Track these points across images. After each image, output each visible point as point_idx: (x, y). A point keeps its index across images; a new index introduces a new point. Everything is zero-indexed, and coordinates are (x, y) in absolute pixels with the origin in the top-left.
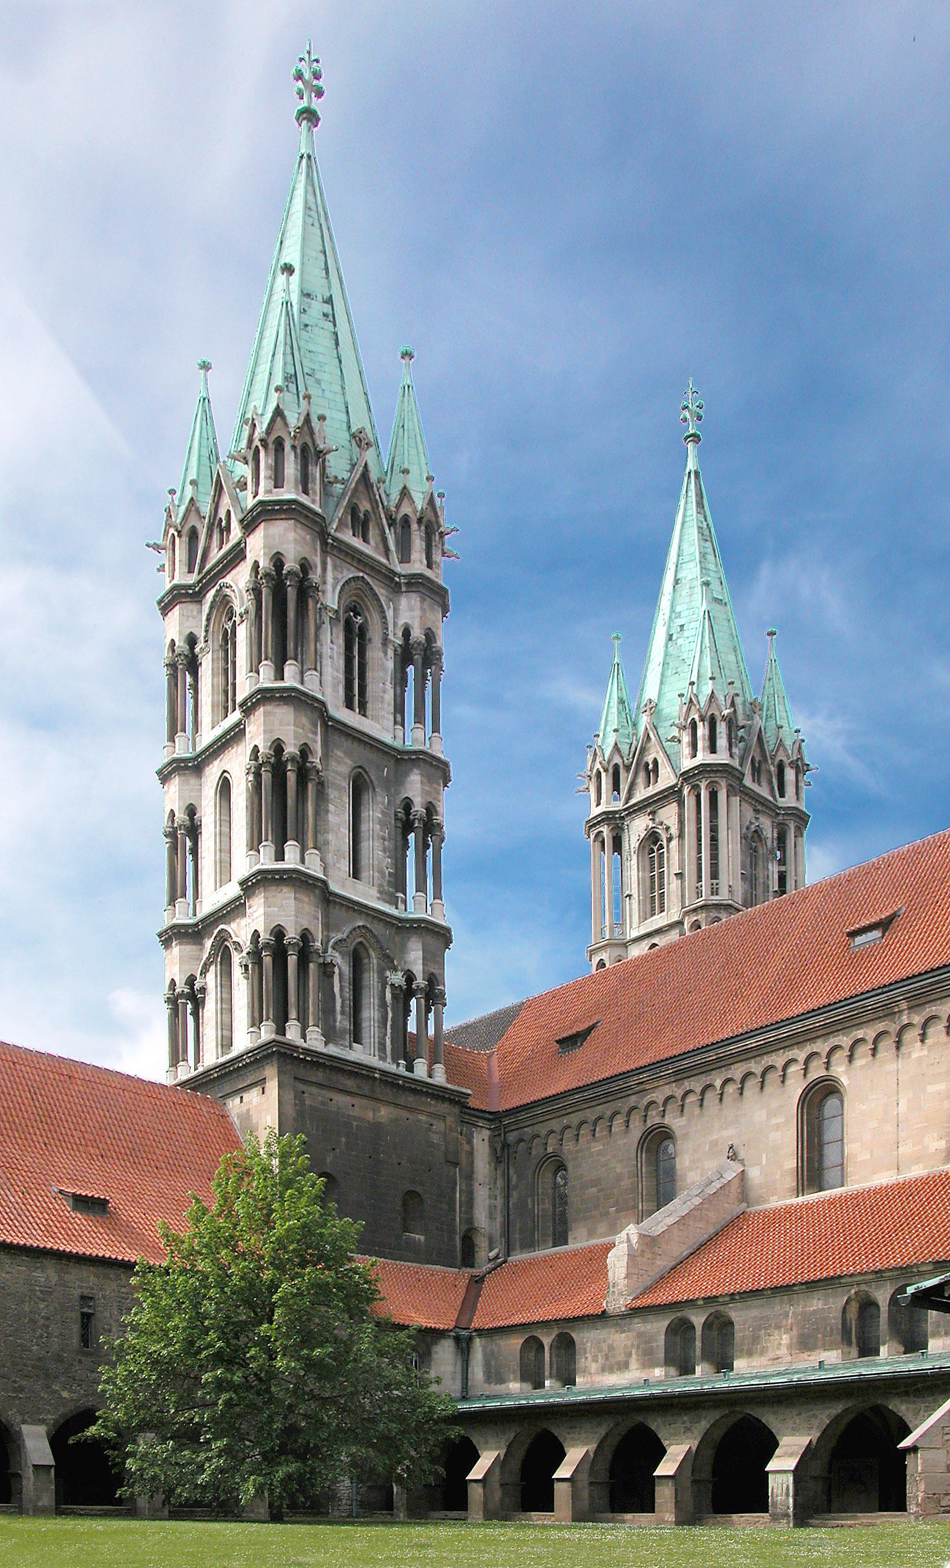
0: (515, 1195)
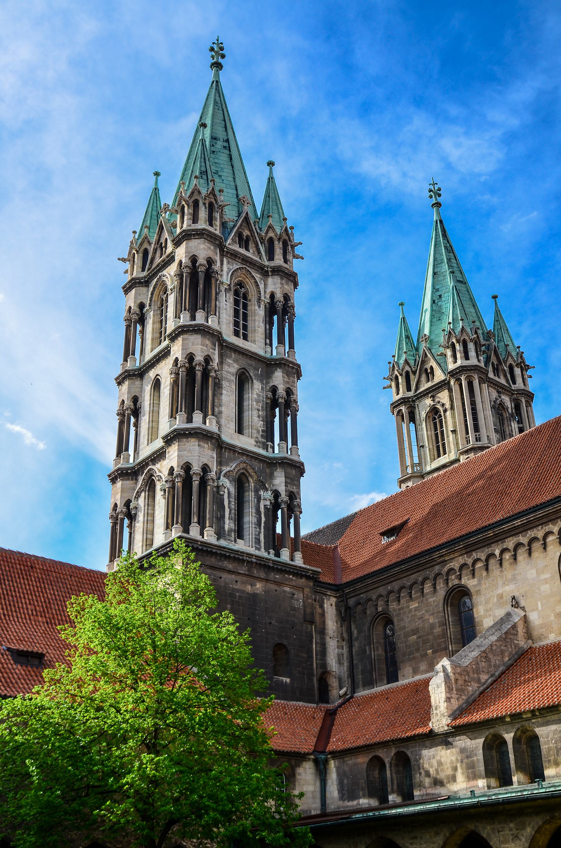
0: (356, 644)
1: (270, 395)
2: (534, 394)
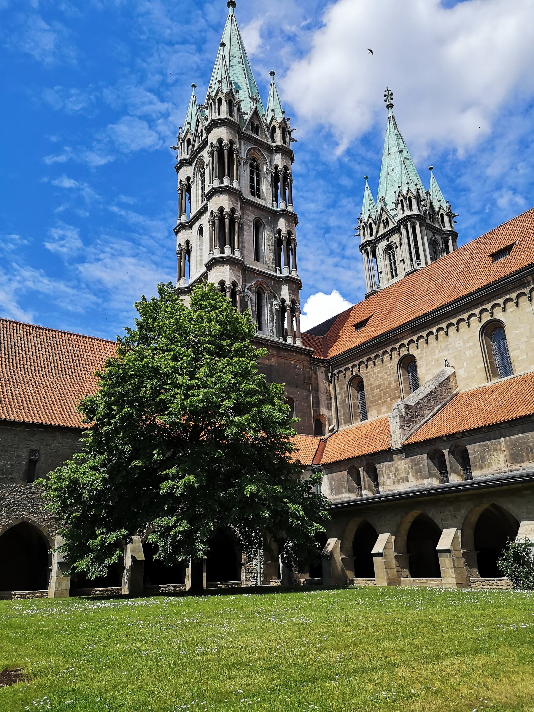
0: (339, 397)
1: (277, 235)
2: (458, 234)
